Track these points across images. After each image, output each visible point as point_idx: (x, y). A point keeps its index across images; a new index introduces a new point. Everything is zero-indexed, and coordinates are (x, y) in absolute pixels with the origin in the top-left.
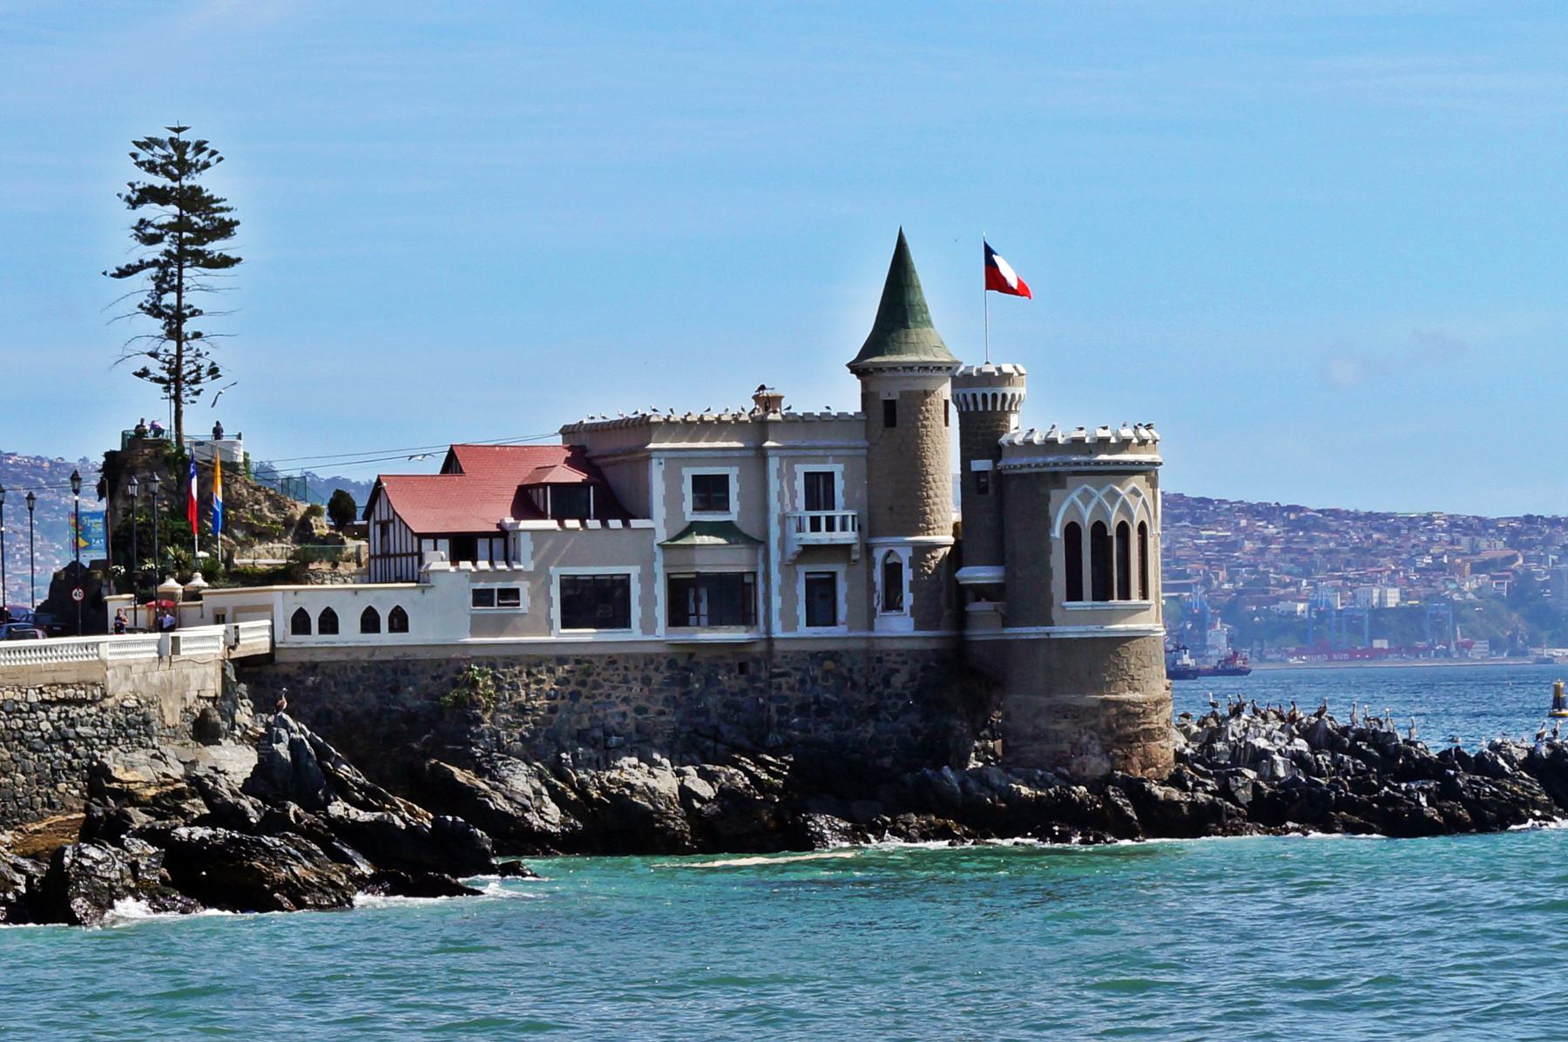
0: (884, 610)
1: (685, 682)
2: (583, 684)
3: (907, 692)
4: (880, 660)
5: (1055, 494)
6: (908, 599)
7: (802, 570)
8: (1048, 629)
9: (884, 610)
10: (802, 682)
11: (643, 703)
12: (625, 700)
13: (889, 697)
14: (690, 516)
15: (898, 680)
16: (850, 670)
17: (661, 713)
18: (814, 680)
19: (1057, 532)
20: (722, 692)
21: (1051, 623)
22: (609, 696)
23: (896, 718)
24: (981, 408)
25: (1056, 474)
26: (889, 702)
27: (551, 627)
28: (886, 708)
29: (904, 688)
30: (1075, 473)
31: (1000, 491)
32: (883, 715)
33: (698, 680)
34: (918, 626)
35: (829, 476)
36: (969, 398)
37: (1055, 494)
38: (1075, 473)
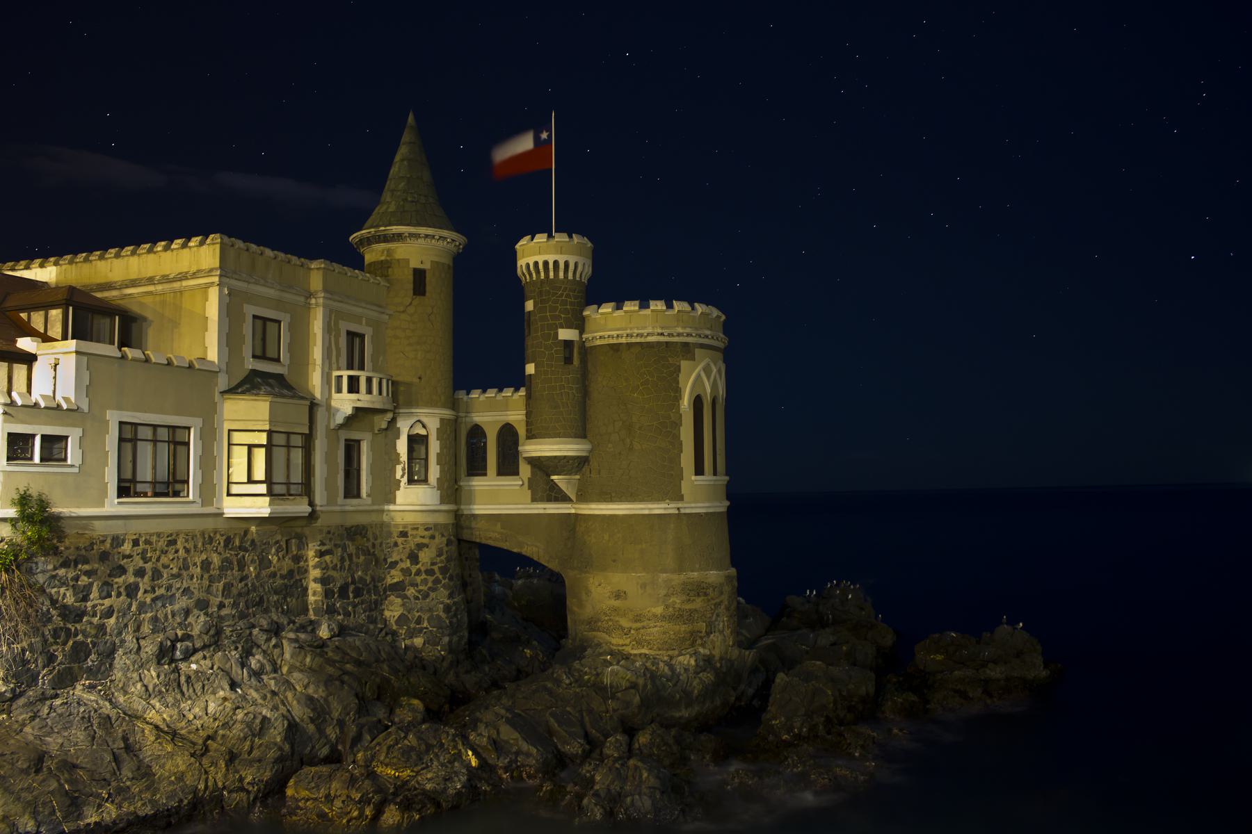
0: (411, 481)
1: (242, 565)
2: (140, 573)
3: (436, 568)
4: (404, 534)
5: (685, 364)
6: (434, 472)
7: (344, 435)
8: (680, 505)
9: (411, 481)
10: (342, 560)
11: (203, 595)
12: (186, 591)
13: (418, 573)
14: (251, 364)
15: (425, 556)
16: (374, 546)
17: (221, 606)
18: (350, 556)
19: (686, 402)
20: (274, 575)
21: (680, 498)
22: (169, 588)
23: (426, 596)
24: (551, 274)
25: (686, 344)
26: (419, 579)
27: (104, 493)
28: (414, 585)
29: (433, 564)
30: (702, 346)
31: (584, 362)
32: (411, 592)
33: (253, 561)
34: (443, 501)
35: (362, 337)
36: (562, 266)
37: (685, 364)
38: (702, 346)
